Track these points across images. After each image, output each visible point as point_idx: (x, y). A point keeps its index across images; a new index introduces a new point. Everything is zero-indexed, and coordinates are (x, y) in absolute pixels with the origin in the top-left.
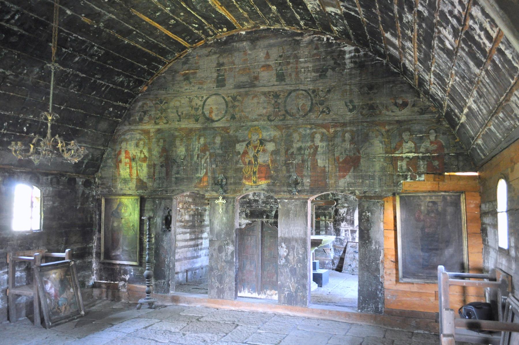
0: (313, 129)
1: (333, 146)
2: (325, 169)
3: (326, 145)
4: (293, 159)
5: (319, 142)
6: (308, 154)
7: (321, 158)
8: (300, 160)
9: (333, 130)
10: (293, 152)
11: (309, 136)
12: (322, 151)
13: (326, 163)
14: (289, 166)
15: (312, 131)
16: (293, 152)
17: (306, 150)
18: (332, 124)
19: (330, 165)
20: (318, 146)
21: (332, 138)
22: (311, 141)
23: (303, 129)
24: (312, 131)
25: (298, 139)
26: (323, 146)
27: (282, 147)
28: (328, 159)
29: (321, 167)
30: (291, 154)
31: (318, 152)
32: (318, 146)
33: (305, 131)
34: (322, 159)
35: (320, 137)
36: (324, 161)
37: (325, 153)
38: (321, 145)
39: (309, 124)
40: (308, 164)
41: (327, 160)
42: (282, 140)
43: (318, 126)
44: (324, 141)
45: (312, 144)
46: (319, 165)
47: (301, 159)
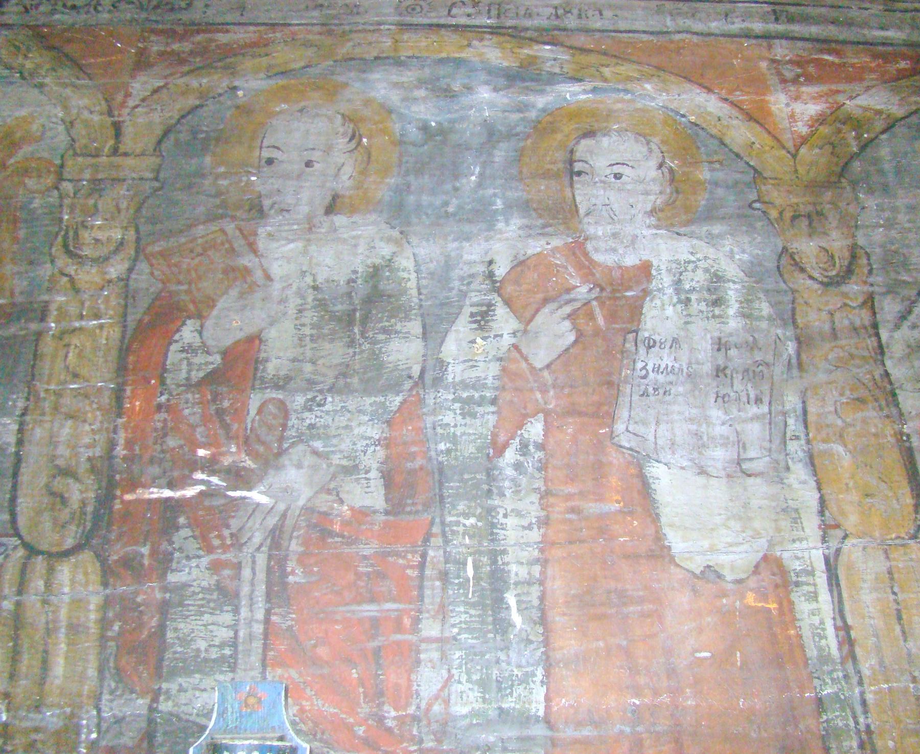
0: (552, 80)
1: (855, 288)
2: (787, 610)
3: (753, 271)
4: (233, 455)
5: (643, 229)
6: (490, 372)
7: (700, 443)
8: (352, 469)
9: (813, 109)
10: (254, 340)
11: (500, 154)
12: (704, 348)
13: (796, 518)
14: (164, 562)
15: (541, 101)
16: (254, 340)
17: (462, 327)
18: (781, 50)
19: (853, 550)
20: (645, 269)
21: (814, 187)
22: (525, 207)
23: (408, 76)
24: (541, 101)
25: (345, 182)
26: (717, 278)
27: (88, 276)
28: (811, 461)
29: (711, 573)
30: (213, 378)
31: (647, 360)
32: (645, 269)
33: (448, 94)
34: (719, 456)
35: (650, 170)
36: (758, 489)
37: (753, 374)
38: (679, 271)
39: (495, 31)
40: (490, 530)
41: (799, 473)
42: (97, 186)
43: (620, 58)
44: (709, 215)
45: (535, 246)
46: (677, 543)
47: (373, 459)
